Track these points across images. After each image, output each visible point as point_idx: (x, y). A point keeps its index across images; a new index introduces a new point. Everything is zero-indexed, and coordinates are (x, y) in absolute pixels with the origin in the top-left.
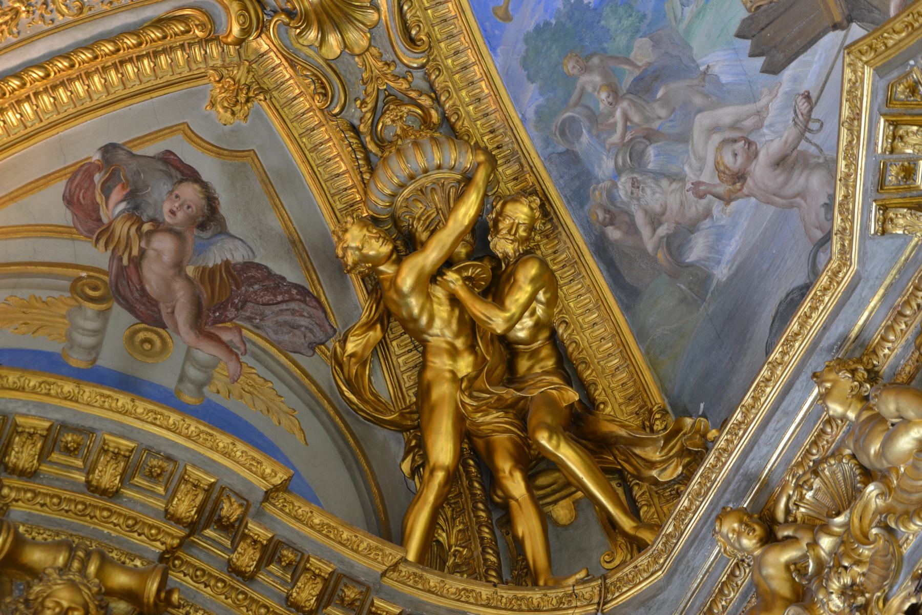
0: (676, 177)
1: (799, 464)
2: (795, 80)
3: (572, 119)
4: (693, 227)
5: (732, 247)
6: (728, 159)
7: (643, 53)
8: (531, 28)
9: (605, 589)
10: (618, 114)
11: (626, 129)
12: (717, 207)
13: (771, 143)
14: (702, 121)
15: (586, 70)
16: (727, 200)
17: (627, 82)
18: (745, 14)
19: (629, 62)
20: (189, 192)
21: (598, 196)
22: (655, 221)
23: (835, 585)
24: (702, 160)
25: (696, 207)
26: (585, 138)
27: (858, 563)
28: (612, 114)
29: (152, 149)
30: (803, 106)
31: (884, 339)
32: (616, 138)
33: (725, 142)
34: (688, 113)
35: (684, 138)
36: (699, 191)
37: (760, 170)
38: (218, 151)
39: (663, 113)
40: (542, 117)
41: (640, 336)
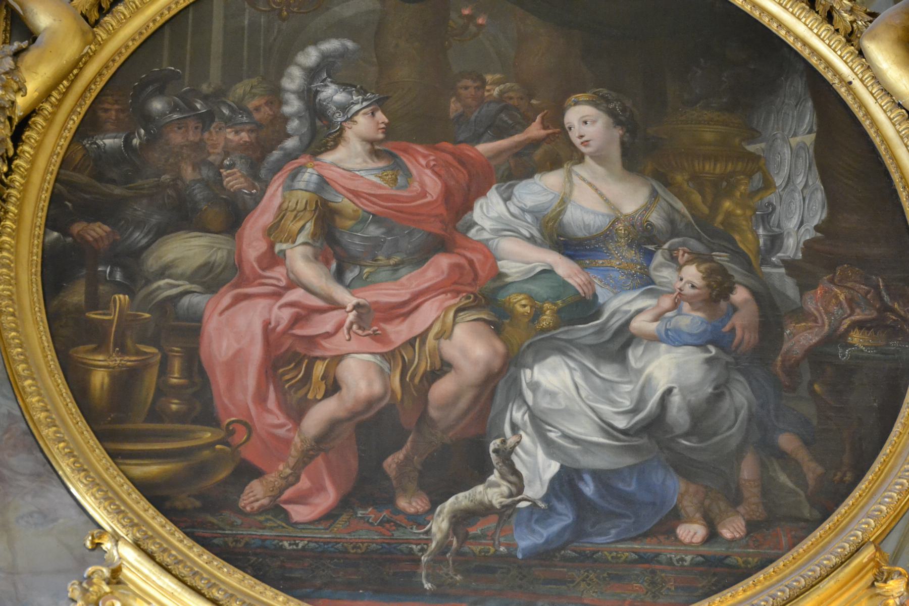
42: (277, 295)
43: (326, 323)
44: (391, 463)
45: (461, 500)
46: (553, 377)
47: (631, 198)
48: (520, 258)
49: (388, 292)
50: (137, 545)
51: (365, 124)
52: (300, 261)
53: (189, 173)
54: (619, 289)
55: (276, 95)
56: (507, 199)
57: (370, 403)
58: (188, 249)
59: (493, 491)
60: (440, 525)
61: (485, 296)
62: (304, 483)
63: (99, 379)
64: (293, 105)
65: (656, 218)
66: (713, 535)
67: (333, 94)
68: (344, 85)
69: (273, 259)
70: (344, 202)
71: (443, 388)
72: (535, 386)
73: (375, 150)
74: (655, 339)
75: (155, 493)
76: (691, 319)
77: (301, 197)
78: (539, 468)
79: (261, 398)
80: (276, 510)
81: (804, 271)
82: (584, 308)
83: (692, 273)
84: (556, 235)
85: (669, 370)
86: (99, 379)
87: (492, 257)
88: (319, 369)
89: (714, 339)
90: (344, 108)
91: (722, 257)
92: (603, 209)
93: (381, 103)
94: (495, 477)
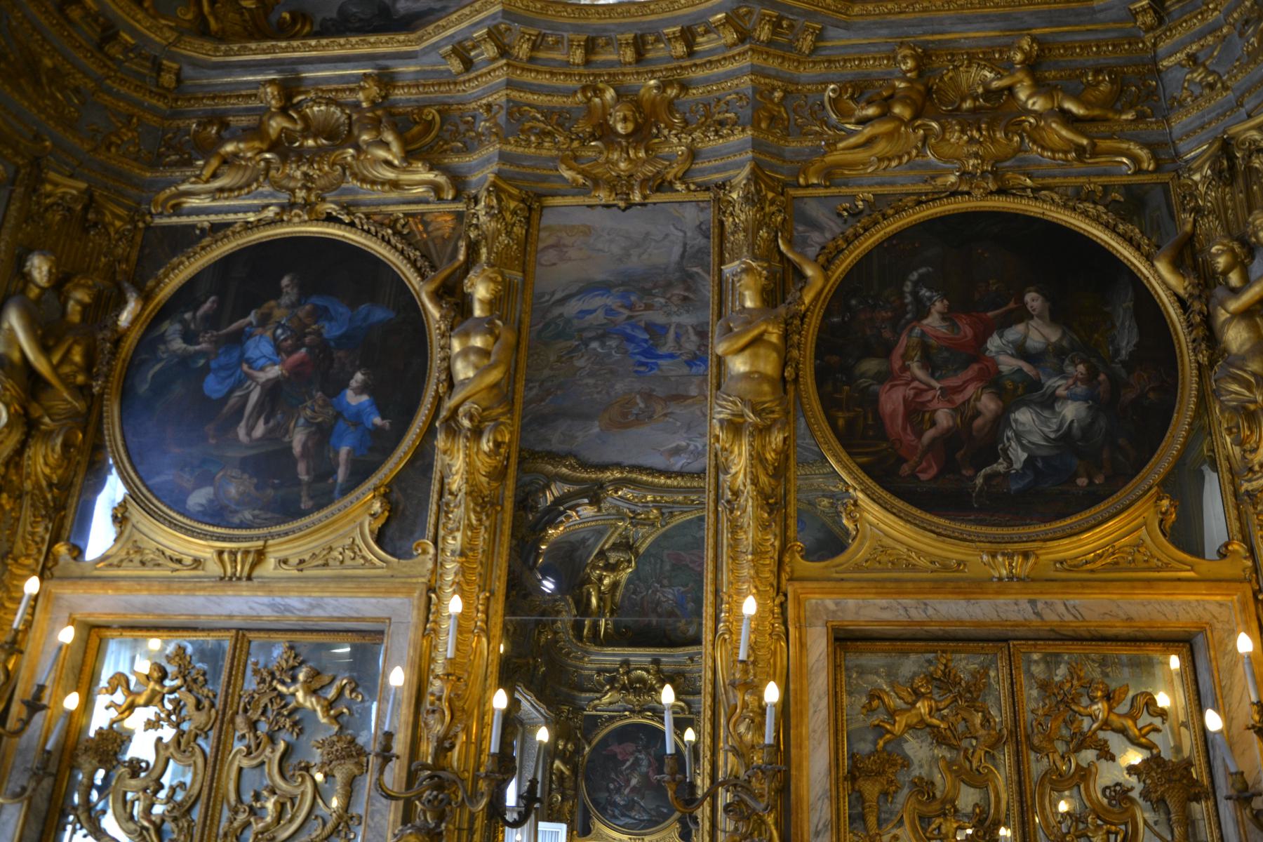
1: (323, 91)
23: (304, 168)
27: (320, 170)
31: (403, 87)
42: (907, 384)
43: (928, 396)
44: (958, 456)
45: (988, 470)
46: (1024, 416)
47: (1054, 335)
48: (1008, 364)
49: (953, 382)
50: (862, 491)
52: (916, 370)
53: (868, 332)
54: (1050, 376)
55: (901, 295)
56: (1001, 337)
57: (949, 430)
58: (870, 366)
59: (1001, 467)
60: (979, 481)
61: (993, 380)
62: (924, 464)
63: (841, 422)
64: (909, 299)
65: (1065, 343)
66: (1091, 483)
67: (925, 292)
68: (930, 289)
69: (905, 368)
70: (933, 342)
71: (978, 422)
72: (1016, 421)
73: (944, 317)
74: (1065, 398)
76: (1081, 389)
77: (915, 340)
78: (1019, 456)
79: (904, 429)
80: (914, 476)
82: (1035, 385)
83: (1081, 368)
84: (1021, 351)
85: (1071, 411)
86: (841, 422)
87: (995, 364)
88: (927, 416)
90: (930, 299)
91: (1093, 360)
92: (1042, 340)
93: (945, 296)
94: (1001, 460)
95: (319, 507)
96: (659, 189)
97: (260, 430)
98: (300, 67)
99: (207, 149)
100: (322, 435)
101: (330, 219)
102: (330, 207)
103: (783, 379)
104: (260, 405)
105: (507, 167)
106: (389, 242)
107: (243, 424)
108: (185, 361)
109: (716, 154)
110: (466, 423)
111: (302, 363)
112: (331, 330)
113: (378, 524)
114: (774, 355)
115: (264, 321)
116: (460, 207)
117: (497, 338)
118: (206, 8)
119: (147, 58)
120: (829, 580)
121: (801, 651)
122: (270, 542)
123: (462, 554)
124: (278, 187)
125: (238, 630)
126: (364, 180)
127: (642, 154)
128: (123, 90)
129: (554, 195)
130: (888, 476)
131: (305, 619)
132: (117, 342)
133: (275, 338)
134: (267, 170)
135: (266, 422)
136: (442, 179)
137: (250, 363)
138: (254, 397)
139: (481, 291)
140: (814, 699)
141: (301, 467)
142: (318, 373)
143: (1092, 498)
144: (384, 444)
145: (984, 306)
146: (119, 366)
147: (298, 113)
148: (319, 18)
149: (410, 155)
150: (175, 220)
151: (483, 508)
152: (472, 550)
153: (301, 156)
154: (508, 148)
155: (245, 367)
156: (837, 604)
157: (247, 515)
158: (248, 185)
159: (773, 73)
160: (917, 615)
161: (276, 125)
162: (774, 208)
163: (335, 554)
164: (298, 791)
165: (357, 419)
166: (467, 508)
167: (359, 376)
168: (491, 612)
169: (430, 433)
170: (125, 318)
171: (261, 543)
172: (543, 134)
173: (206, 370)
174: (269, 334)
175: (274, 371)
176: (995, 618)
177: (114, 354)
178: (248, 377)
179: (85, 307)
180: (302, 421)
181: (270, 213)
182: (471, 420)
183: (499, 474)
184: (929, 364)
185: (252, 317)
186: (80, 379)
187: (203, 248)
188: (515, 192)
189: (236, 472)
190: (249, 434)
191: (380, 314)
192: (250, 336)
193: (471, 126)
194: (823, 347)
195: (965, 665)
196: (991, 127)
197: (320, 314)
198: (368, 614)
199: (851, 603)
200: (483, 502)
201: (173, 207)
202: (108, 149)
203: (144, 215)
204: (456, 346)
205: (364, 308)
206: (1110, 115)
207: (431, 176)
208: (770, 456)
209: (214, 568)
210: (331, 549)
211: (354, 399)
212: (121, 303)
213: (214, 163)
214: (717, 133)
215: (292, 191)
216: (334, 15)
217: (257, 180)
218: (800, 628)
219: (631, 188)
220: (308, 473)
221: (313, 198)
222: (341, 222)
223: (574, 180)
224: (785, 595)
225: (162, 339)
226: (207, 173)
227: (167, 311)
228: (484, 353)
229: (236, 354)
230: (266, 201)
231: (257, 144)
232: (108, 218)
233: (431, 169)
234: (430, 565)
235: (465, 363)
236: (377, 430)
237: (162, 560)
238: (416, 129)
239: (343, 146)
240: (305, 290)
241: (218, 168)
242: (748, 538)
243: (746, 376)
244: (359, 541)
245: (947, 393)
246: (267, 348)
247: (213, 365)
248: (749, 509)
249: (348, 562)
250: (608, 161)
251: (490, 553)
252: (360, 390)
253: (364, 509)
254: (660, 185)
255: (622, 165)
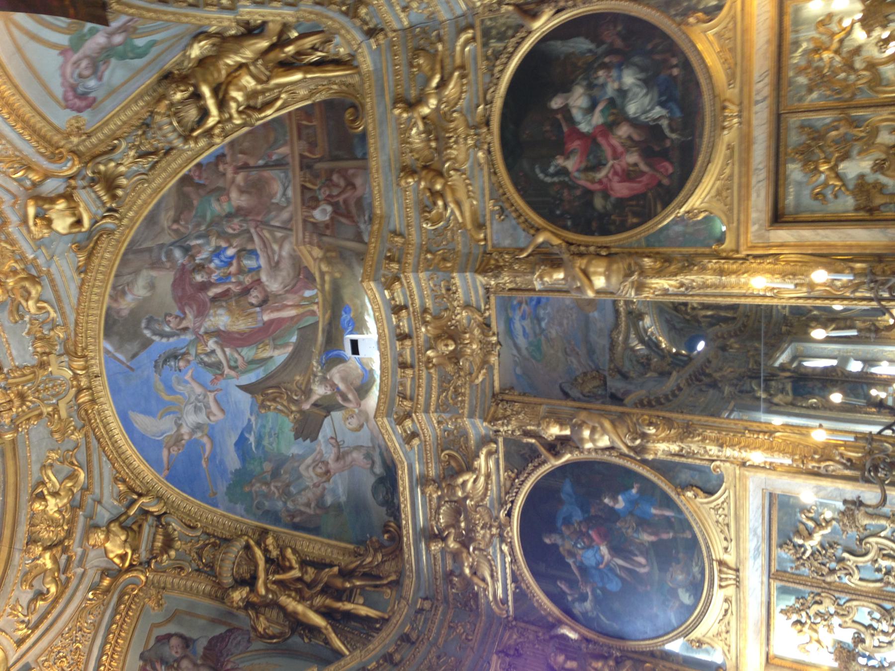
0: (307, 487)
2: (324, 437)
3: (258, 503)
4: (322, 496)
5: (341, 490)
6: (319, 471)
7: (268, 466)
8: (225, 489)
9: (405, 598)
10: (273, 488)
11: (278, 490)
12: (326, 485)
13: (330, 455)
14: (302, 468)
15: (252, 486)
16: (329, 480)
17: (269, 478)
18: (293, 433)
19: (264, 472)
20: (174, 641)
21: (283, 514)
22: (308, 505)
23: (479, 529)
24: (311, 478)
25: (318, 491)
26: (267, 503)
28: (270, 490)
29: (152, 642)
30: (333, 441)
31: (428, 471)
32: (277, 495)
33: (314, 468)
34: (296, 469)
35: (300, 476)
36: (315, 485)
37: (332, 465)
38: (168, 621)
39: (287, 476)
40: (248, 511)
41: (329, 537)
42: (610, 180)
43: (618, 168)
44: (657, 149)
45: (667, 131)
46: (632, 109)
48: (597, 119)
49: (608, 152)
50: (680, 208)
51: (560, 161)
53: (576, 204)
54: (606, 93)
55: (553, 184)
56: (579, 123)
57: (640, 155)
58: (598, 203)
59: (664, 123)
60: (674, 136)
61: (608, 128)
62: (662, 170)
63: (635, 220)
64: (556, 179)
65: (585, 83)
66: (676, 66)
67: (552, 170)
68: (549, 166)
69: (600, 182)
70: (583, 165)
71: (636, 137)
72: (635, 113)
73: (567, 158)
74: (621, 83)
75: (665, 205)
76: (614, 73)
77: (582, 176)
78: (658, 111)
79: (639, 182)
80: (670, 176)
81: (598, 42)
82: (612, 102)
83: (601, 73)
84: (590, 110)
85: (629, 79)
86: (635, 220)
87: (597, 127)
88: (631, 168)
89: (620, 66)
90: (556, 166)
91: (596, 65)
92: (582, 98)
93: (553, 157)
94: (660, 123)
95: (690, 528)
96: (488, 326)
97: (641, 560)
98: (418, 529)
99: (468, 583)
100: (644, 523)
101: (509, 514)
102: (502, 514)
103: (607, 256)
104: (625, 559)
105: (477, 414)
106: (523, 481)
107: (637, 569)
108: (597, 601)
109: (467, 293)
110: (638, 442)
111: (599, 534)
112: (578, 516)
113: (701, 493)
114: (594, 262)
115: (572, 554)
116: (500, 440)
117: (584, 422)
118: (385, 582)
119: (416, 617)
120: (738, 229)
121: (787, 246)
122: (714, 557)
123: (721, 446)
124: (490, 543)
125: (769, 577)
126: (485, 495)
127: (467, 336)
128: (434, 630)
129: (493, 387)
130: (669, 193)
131: (763, 539)
132: (588, 641)
133: (583, 548)
134: (480, 550)
135: (636, 555)
136: (484, 451)
137: (598, 563)
138: (620, 562)
139: (555, 431)
140: (818, 238)
141: (665, 536)
142: (605, 524)
143: (686, 65)
144: (648, 488)
145: (561, 134)
146: (602, 640)
147: (444, 531)
148: (387, 518)
149: (470, 468)
150: (510, 603)
151: (690, 433)
152: (718, 440)
153: (471, 530)
154: (466, 411)
155: (601, 566)
156: (754, 224)
157: (696, 570)
158: (489, 561)
159: (416, 259)
160: (763, 175)
161: (452, 545)
162: (501, 260)
163: (721, 519)
164: (875, 547)
165: (633, 503)
166: (692, 442)
167: (606, 501)
168: (758, 429)
169: (644, 462)
170: (573, 635)
171: (715, 563)
172: (457, 393)
173: (603, 589)
174: (580, 552)
175: (604, 550)
176: (766, 126)
177: (595, 643)
178: (607, 565)
179: (568, 658)
180: (635, 535)
181: (505, 548)
182: (636, 439)
183: (669, 423)
184: (598, 166)
185: (570, 561)
186: (611, 663)
187: (528, 588)
188: (492, 409)
189: (668, 575)
190: (644, 566)
191: (567, 487)
192: (582, 562)
193: (450, 432)
194: (587, 231)
195: (794, 138)
196: (447, 131)
197: (567, 521)
198: (760, 502)
199: (754, 215)
200: (687, 432)
201: (503, 604)
202: (469, 640)
203: (509, 622)
204: (589, 445)
205: (563, 496)
206: (439, 58)
207: (483, 457)
208: (658, 265)
209: (730, 591)
210: (717, 522)
211: (621, 504)
212: (565, 637)
213: (476, 580)
214: (454, 293)
215: (492, 536)
216: (384, 509)
217: (486, 556)
218: (770, 247)
219: (489, 342)
220: (668, 533)
221: (496, 524)
222: (511, 508)
223: (484, 374)
224: (748, 255)
225: (584, 614)
226: (482, 585)
227: (568, 612)
228: (593, 431)
229: (593, 571)
230: (498, 550)
231: (465, 555)
232: (512, 642)
233: (478, 457)
234: (728, 464)
235: (599, 440)
236: (640, 491)
237: (726, 620)
238: (453, 463)
239: (465, 506)
240: (553, 529)
241: (479, 578)
242: (711, 279)
243: (608, 278)
244: (712, 505)
245: (616, 156)
246: (589, 554)
247: (600, 585)
248: (693, 277)
249: (726, 512)
250: (472, 355)
251: (720, 430)
252: (616, 500)
253: (692, 503)
254: (486, 324)
255: (474, 346)
